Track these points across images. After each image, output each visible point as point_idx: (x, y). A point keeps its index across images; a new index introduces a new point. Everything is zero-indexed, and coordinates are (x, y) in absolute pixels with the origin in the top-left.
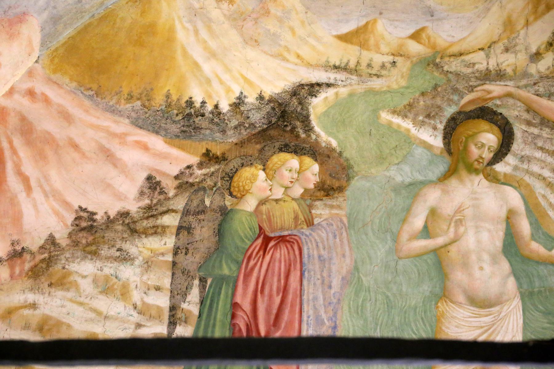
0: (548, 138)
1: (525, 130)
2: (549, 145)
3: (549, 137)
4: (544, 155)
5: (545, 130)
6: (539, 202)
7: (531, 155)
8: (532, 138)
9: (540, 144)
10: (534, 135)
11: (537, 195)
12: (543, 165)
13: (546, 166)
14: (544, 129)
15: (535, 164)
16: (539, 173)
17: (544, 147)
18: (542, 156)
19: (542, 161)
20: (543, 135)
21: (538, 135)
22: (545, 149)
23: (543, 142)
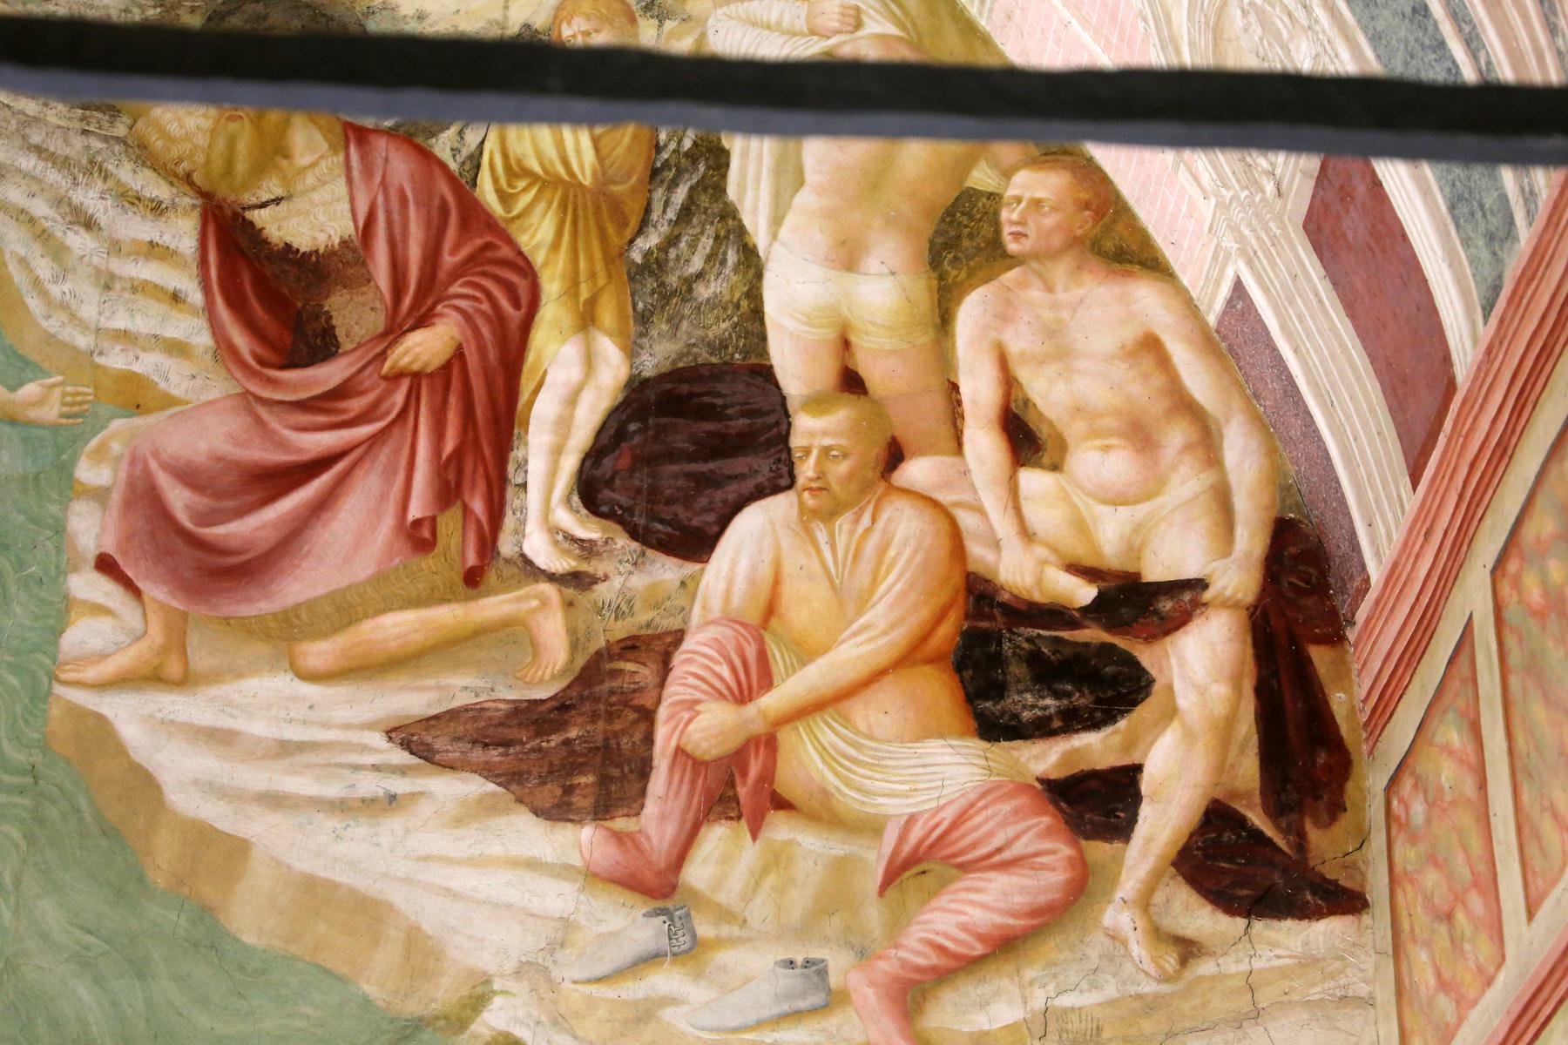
0: (59, 127)
1: (6, 102)
2: (60, 143)
3: (62, 124)
4: (41, 164)
5: (56, 108)
6: (8, 274)
7: (9, 162)
8: (17, 123)
9: (36, 138)
10: (25, 114)
11: (7, 256)
12: (35, 188)
13: (42, 190)
14: (53, 104)
15: (15, 183)
16: (21, 207)
17: (44, 146)
18: (35, 167)
19: (33, 178)
20: (48, 118)
21: (35, 118)
22: (47, 150)
23: (44, 134)
